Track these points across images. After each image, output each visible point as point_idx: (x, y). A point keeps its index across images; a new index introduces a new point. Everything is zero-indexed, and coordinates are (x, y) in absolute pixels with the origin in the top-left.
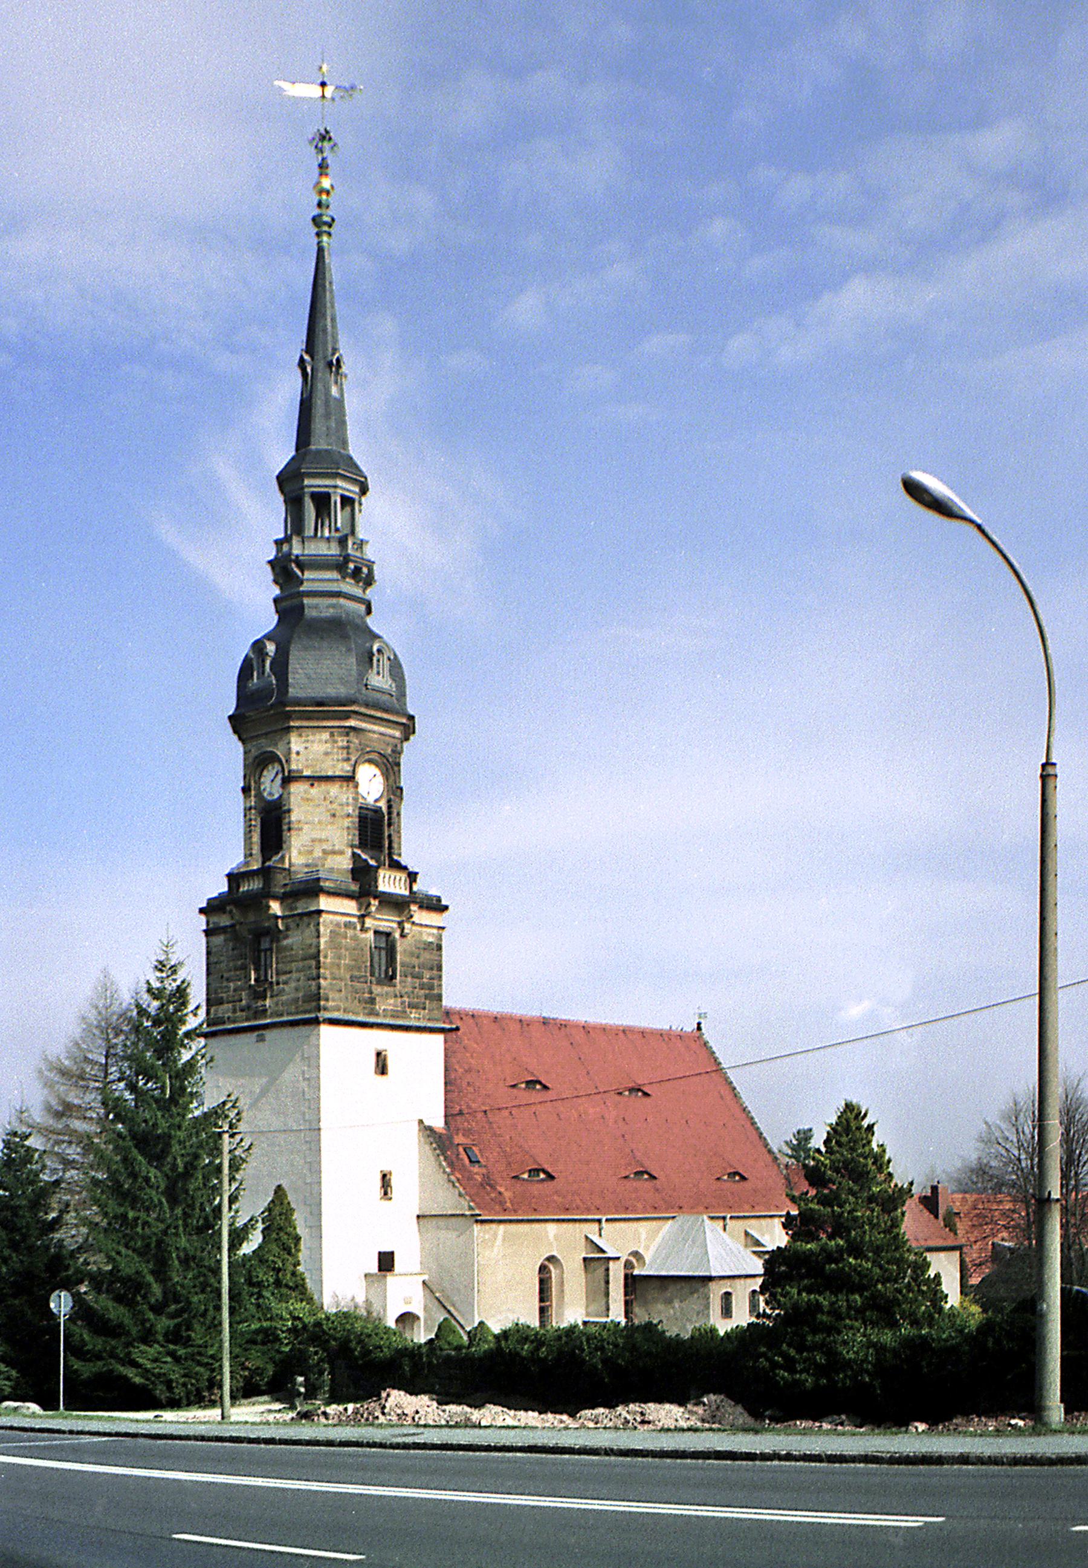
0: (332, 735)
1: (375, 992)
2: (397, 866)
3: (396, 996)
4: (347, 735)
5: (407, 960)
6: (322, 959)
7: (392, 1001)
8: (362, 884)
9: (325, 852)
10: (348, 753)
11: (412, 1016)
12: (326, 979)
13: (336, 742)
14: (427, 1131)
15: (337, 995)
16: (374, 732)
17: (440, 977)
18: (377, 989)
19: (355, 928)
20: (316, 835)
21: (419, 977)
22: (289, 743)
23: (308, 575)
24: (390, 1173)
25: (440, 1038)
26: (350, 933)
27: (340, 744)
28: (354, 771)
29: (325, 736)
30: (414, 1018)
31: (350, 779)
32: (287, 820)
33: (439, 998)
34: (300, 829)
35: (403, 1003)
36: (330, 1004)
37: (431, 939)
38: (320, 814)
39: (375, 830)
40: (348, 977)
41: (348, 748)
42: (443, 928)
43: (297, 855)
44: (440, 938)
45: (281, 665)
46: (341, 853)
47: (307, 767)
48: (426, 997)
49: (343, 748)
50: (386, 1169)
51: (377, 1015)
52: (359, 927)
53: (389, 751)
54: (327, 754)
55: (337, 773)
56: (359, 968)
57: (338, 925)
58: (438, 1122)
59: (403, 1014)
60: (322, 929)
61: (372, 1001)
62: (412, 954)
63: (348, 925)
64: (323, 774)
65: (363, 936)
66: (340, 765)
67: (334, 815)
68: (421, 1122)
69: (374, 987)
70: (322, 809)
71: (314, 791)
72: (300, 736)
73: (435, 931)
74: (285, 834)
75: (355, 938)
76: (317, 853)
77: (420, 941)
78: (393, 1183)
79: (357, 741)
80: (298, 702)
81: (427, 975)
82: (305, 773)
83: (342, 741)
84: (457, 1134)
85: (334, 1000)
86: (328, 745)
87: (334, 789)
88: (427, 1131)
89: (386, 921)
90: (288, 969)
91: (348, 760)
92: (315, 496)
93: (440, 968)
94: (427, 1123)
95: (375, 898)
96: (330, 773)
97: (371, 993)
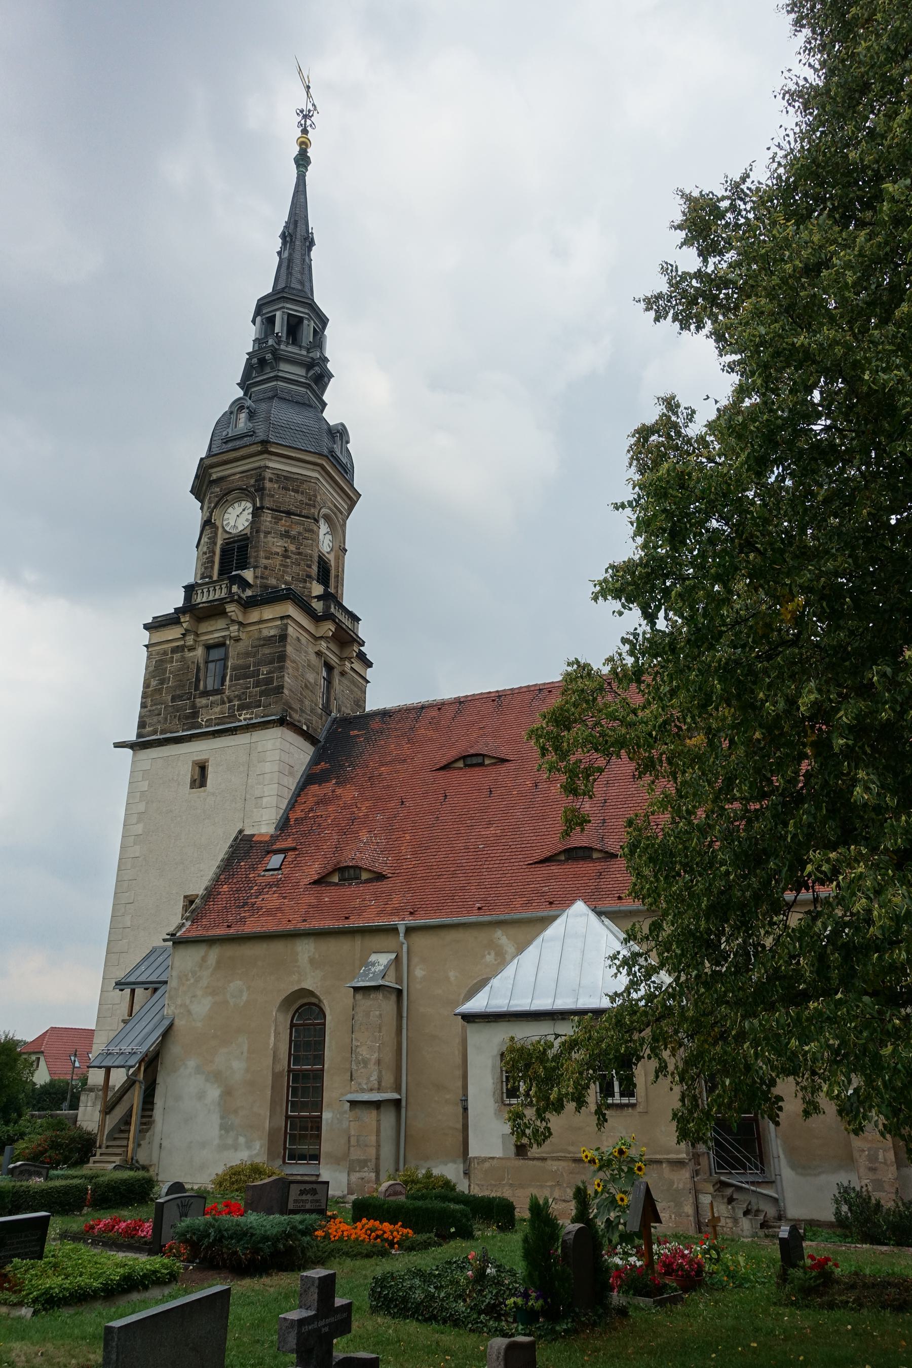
1: (198, 705)
5: (240, 662)
7: (217, 709)
11: (241, 718)
15: (155, 719)
16: (234, 474)
30: (244, 717)
36: (148, 729)
37: (272, 632)
40: (169, 698)
48: (262, 693)
53: (252, 481)
56: (184, 686)
57: (165, 653)
59: (232, 717)
61: (195, 714)
62: (247, 654)
63: (175, 650)
65: (191, 654)
69: (198, 700)
73: (279, 623)
77: (260, 639)
85: (151, 725)
89: (214, 631)
97: (193, 706)
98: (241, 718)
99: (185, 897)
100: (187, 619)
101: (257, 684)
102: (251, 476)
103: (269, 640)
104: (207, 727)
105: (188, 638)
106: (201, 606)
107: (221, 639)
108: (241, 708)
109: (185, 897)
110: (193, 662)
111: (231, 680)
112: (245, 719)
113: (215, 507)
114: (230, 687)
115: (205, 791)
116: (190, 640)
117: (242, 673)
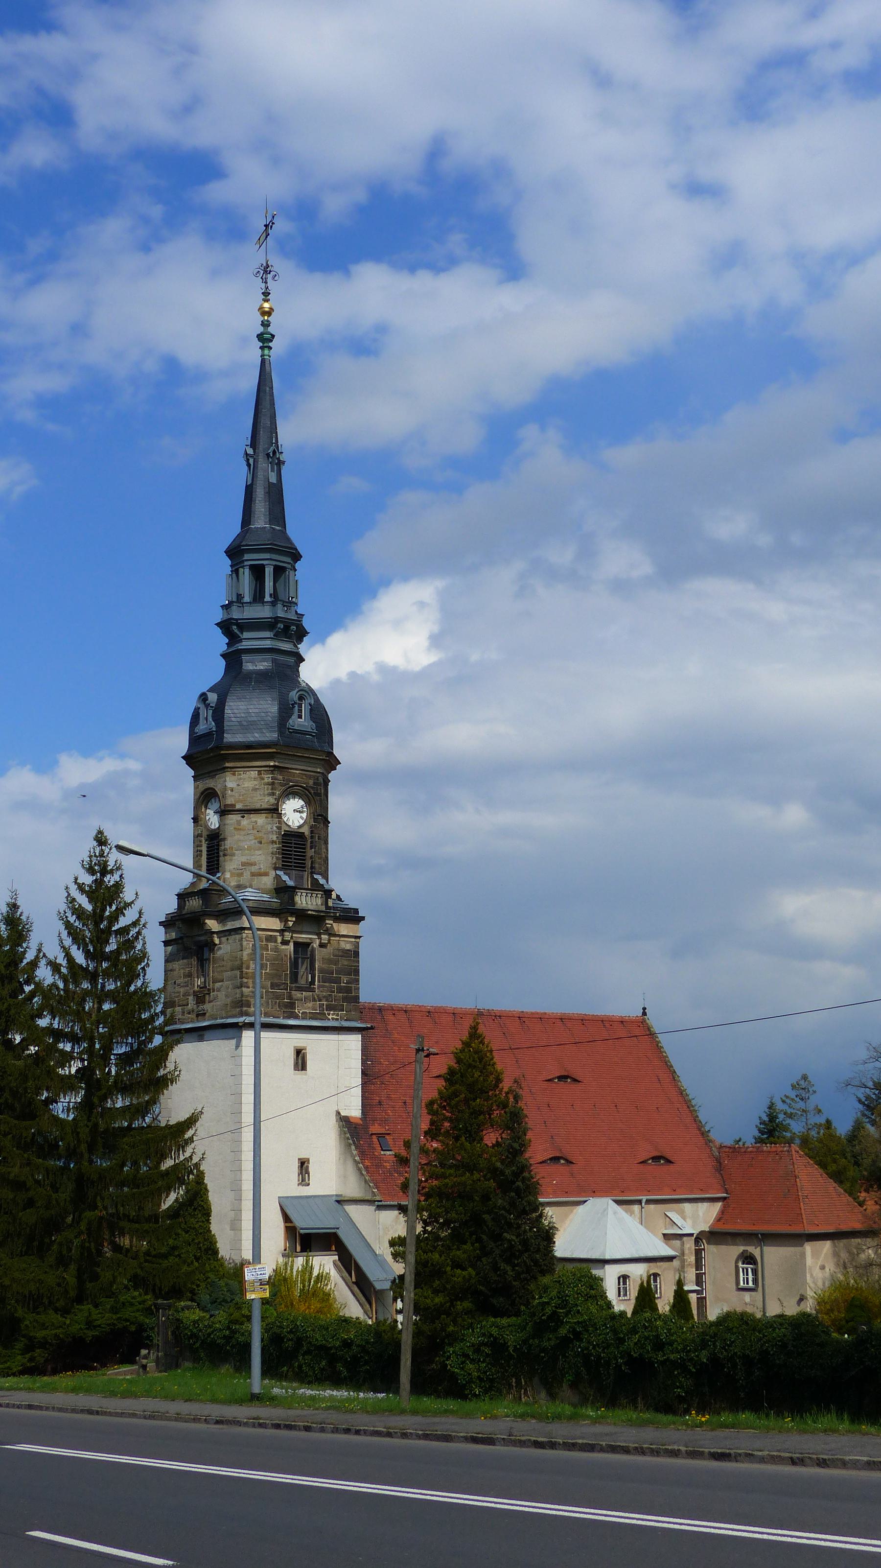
0: (260, 773)
1: (294, 997)
2: (316, 887)
3: (314, 1000)
4: (272, 772)
5: (325, 966)
6: (245, 970)
7: (310, 1005)
8: (282, 904)
9: (253, 874)
10: (272, 789)
11: (330, 1017)
12: (248, 987)
13: (263, 779)
14: (345, 1122)
17: (357, 981)
18: (297, 995)
19: (276, 941)
20: (244, 859)
21: (337, 981)
22: (225, 781)
23: (246, 635)
24: (308, 1160)
25: (359, 1037)
26: (271, 945)
27: (266, 780)
28: (277, 804)
29: (254, 774)
30: (332, 1019)
31: (274, 811)
32: (223, 848)
33: (356, 998)
34: (233, 855)
35: (321, 1006)
38: (249, 842)
39: (302, 853)
41: (273, 784)
42: (359, 937)
43: (228, 877)
44: (357, 945)
45: (219, 713)
46: (266, 874)
47: (238, 802)
48: (345, 999)
49: (268, 784)
50: (303, 1156)
51: (296, 1017)
52: (279, 939)
54: (255, 790)
55: (265, 806)
58: (354, 1111)
60: (245, 943)
61: (292, 1005)
62: (330, 961)
64: (253, 807)
65: (284, 947)
66: (267, 799)
67: (260, 843)
68: (338, 1113)
69: (293, 992)
70: (251, 837)
71: (245, 822)
72: (234, 775)
74: (221, 859)
75: (276, 949)
76: (247, 875)
77: (338, 950)
78: (311, 1170)
79: (281, 777)
80: (232, 746)
81: (345, 979)
82: (238, 806)
83: (268, 778)
84: (373, 1124)
86: (256, 783)
87: (261, 820)
88: (345, 1122)
90: (220, 977)
91: (273, 794)
92: (253, 568)
93: (357, 972)
94: (343, 1114)
95: (292, 915)
96: (258, 806)
97: (290, 997)
98: (330, 1017)
99: (299, 1159)
100: (294, 919)
101: (340, 990)
102: (310, 777)
103: (346, 953)
104: (303, 1019)
105: (286, 934)
106: (310, 912)
107: (308, 941)
108: (330, 1008)
109: (299, 1159)
110: (286, 956)
111: (319, 981)
112: (333, 1019)
113: (280, 797)
114: (319, 987)
115: (306, 1074)
116: (288, 936)
117: (328, 977)
